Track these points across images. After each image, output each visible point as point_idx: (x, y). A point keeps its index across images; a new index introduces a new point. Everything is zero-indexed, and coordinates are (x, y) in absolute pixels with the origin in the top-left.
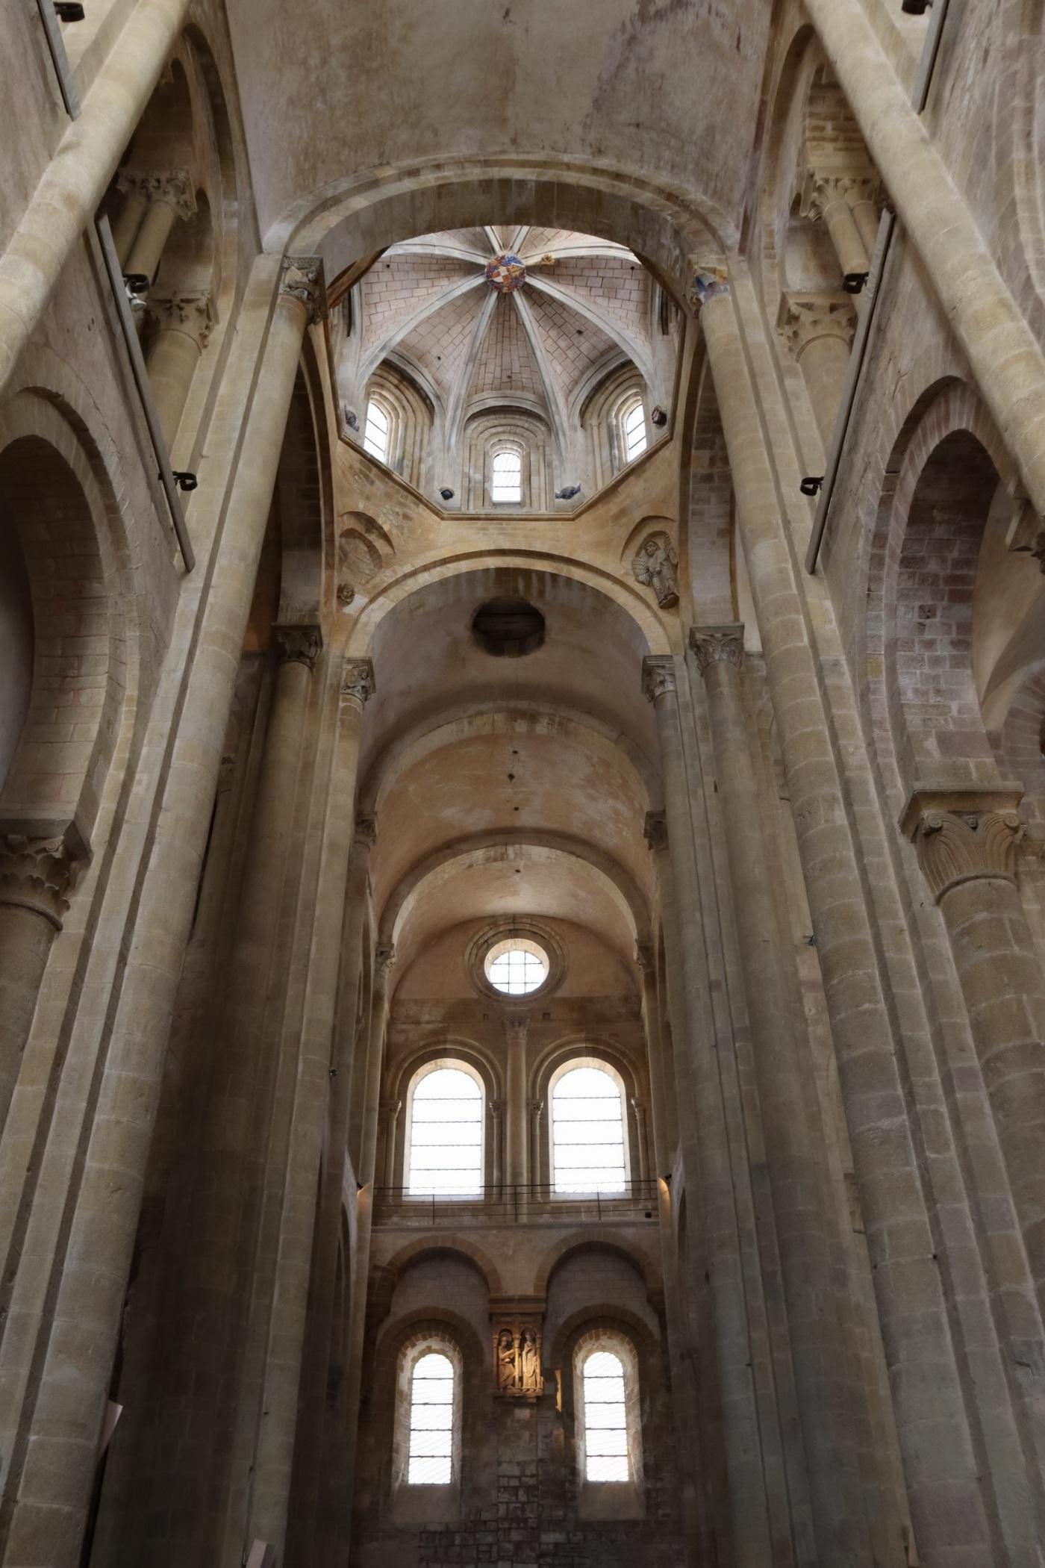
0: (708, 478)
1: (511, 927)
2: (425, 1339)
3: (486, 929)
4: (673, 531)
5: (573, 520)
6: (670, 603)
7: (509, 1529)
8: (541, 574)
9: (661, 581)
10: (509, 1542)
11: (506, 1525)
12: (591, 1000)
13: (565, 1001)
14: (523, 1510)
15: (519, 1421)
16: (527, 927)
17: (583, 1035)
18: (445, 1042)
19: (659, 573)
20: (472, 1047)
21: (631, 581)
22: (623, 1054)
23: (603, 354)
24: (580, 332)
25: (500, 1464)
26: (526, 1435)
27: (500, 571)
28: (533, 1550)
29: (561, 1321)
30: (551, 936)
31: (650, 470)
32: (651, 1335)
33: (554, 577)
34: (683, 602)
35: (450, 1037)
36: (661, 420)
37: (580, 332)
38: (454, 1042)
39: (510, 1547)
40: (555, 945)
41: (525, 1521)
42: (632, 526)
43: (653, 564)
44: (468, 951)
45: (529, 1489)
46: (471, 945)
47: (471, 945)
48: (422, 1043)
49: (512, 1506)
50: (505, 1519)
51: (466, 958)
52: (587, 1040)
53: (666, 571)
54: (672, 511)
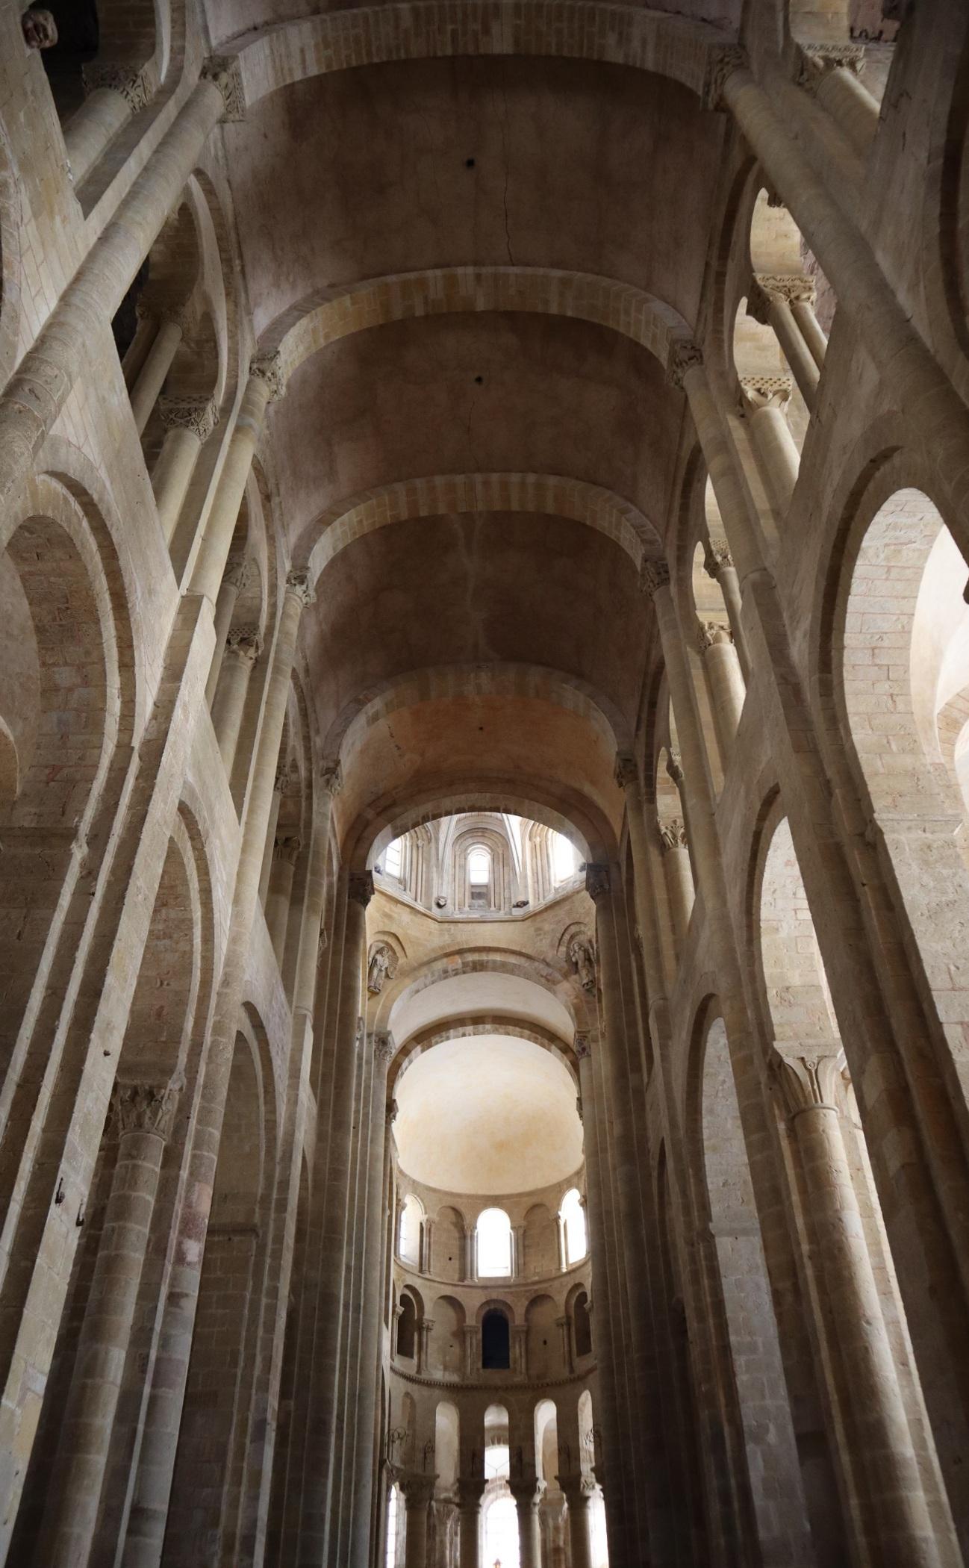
0: (445, 972)
31: (419, 919)
34: (376, 998)
36: (439, 906)
43: (379, 957)
54: (413, 954)
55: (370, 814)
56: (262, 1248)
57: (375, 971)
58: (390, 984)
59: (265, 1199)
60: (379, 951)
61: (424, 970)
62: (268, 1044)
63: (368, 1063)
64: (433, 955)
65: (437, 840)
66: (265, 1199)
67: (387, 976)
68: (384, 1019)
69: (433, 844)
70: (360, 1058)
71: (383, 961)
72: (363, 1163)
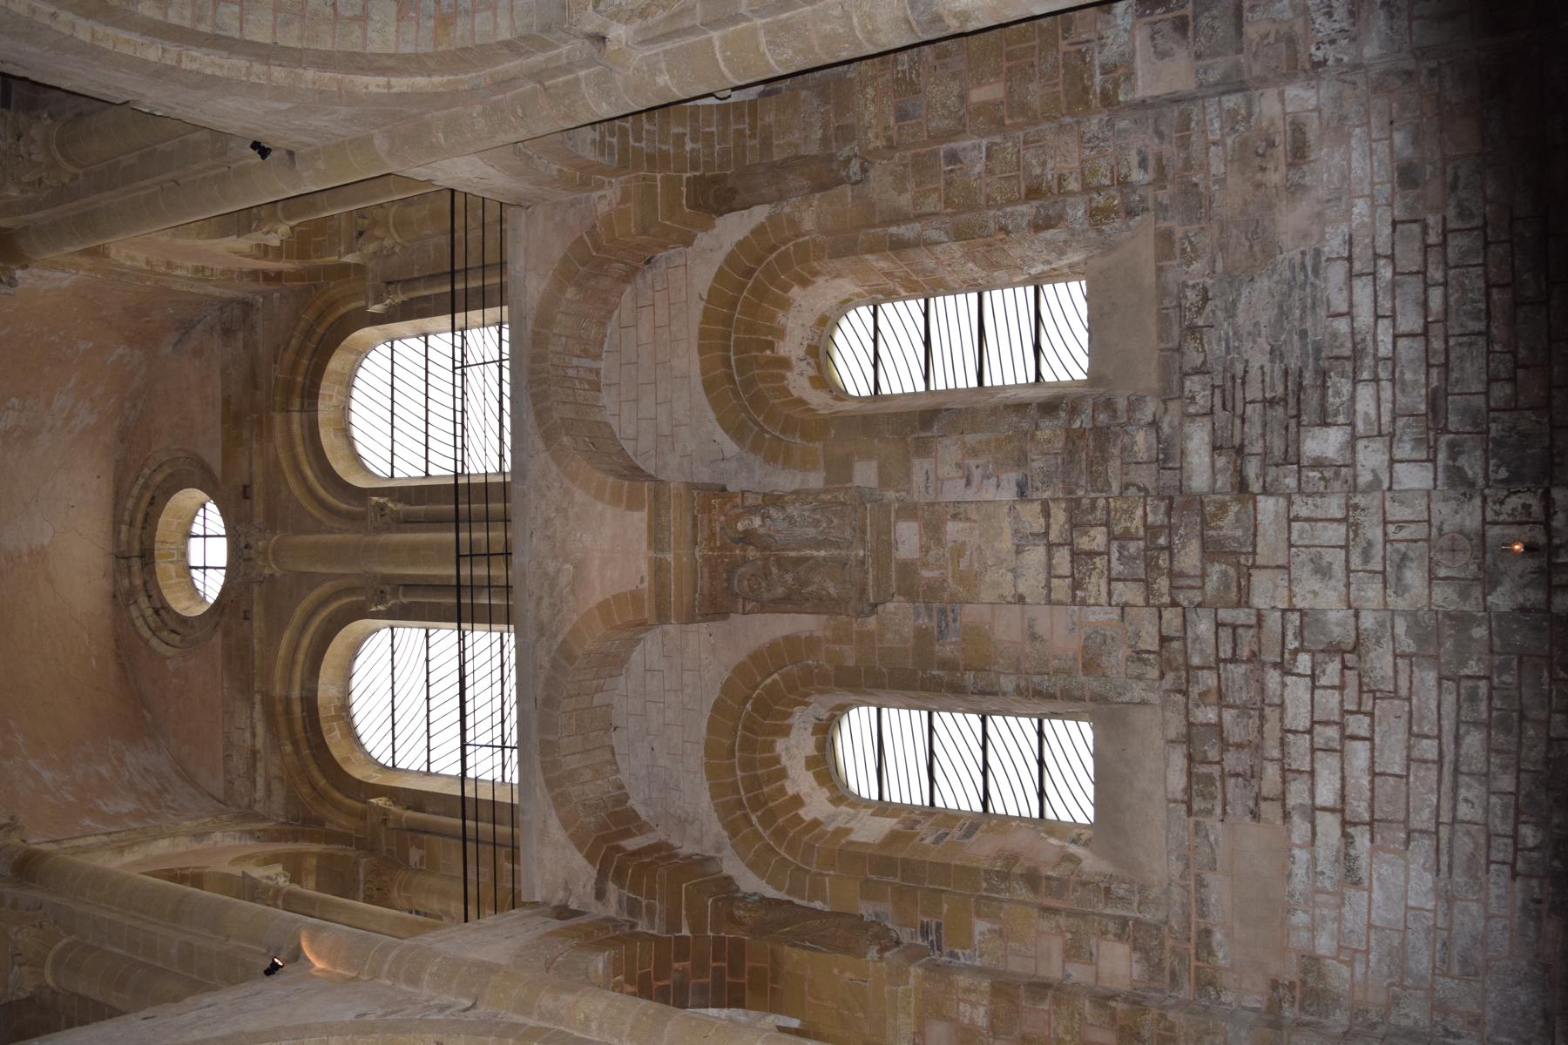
1: (136, 564)
2: (782, 774)
3: (134, 612)
7: (1172, 574)
10: (1204, 575)
11: (1163, 583)
12: (226, 402)
13: (227, 456)
14: (1127, 536)
15: (925, 550)
16: (137, 531)
17: (278, 418)
18: (288, 701)
20: (295, 648)
22: (309, 333)
25: (1021, 599)
26: (952, 527)
28: (1223, 507)
29: (731, 448)
30: (146, 486)
32: (759, 231)
35: (278, 690)
38: (289, 682)
39: (1215, 570)
40: (159, 478)
41: (1151, 531)
44: (163, 649)
45: (1076, 524)
46: (154, 642)
47: (154, 642)
48: (288, 748)
49: (1117, 567)
50: (1148, 584)
51: (169, 651)
52: (286, 409)
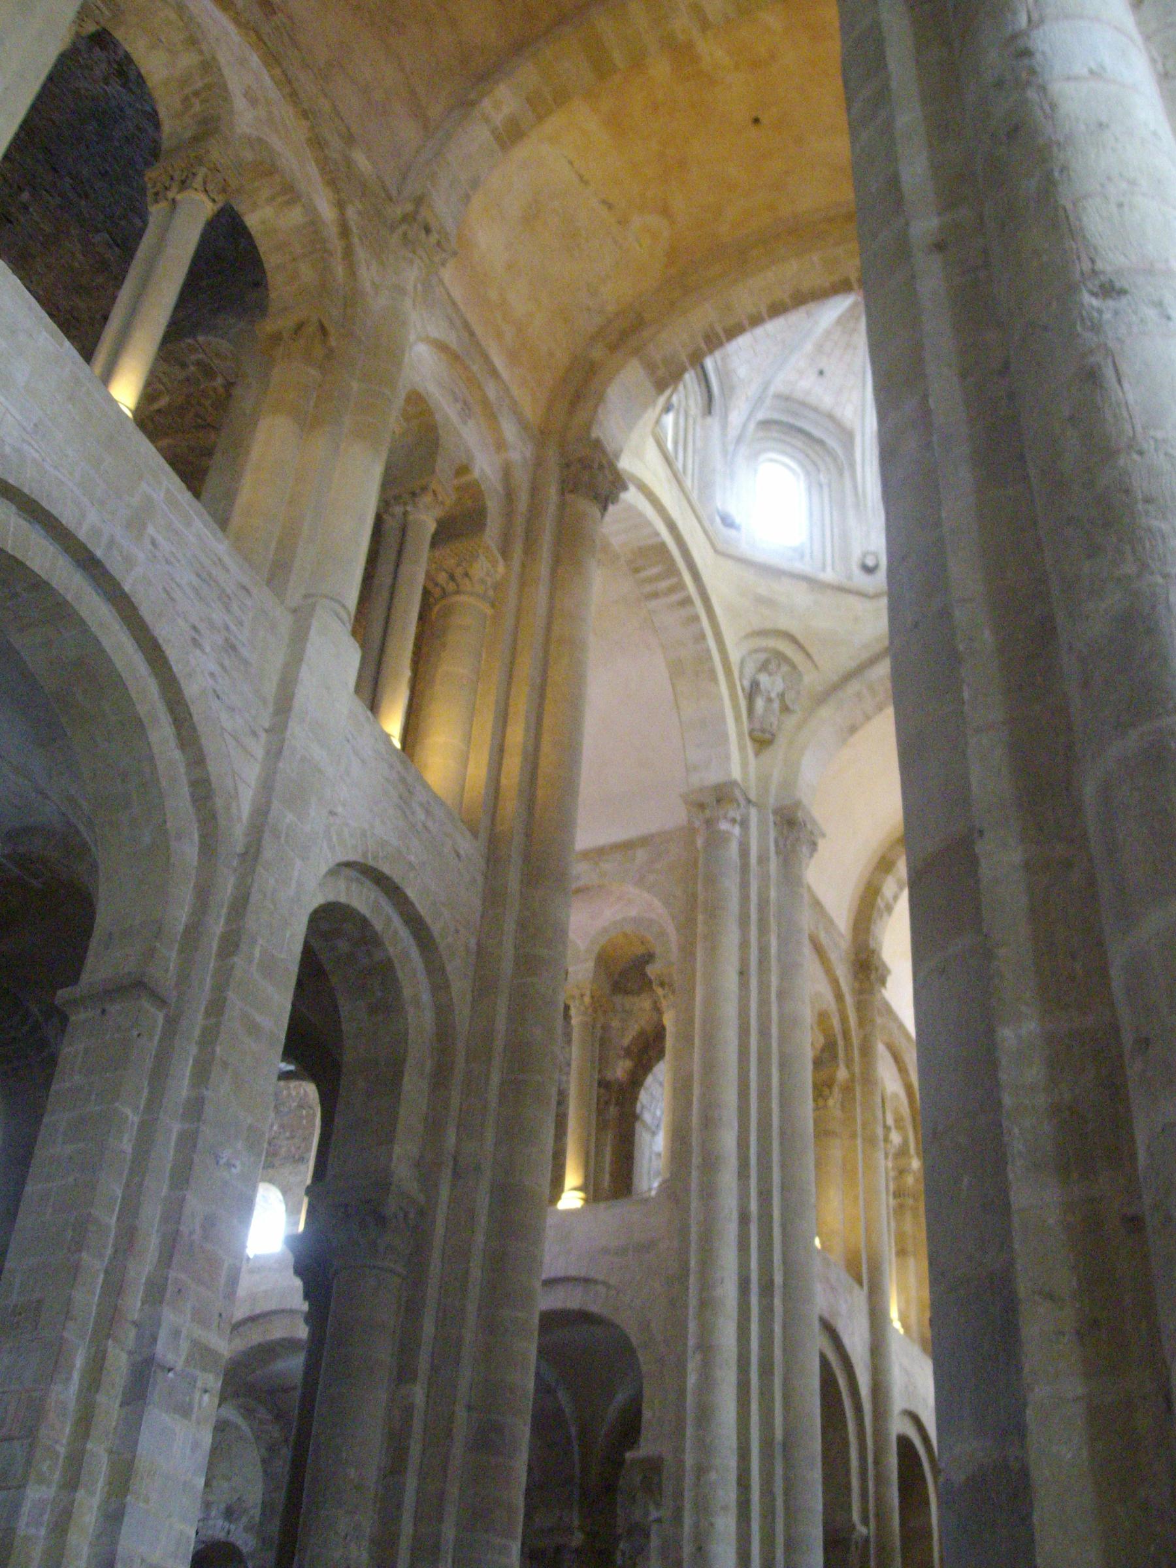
4: (811, 680)
5: (716, 551)
6: (762, 741)
8: (681, 586)
9: (766, 710)
19: (769, 700)
21: (736, 674)
23: (803, 404)
24: (821, 373)
27: (662, 548)
33: (687, 601)
37: (821, 373)
42: (768, 625)
43: (764, 679)
53: (776, 705)
54: (832, 663)
55: (597, 353)
56: (172, 1023)
57: (760, 703)
58: (791, 721)
59: (193, 932)
60: (764, 667)
61: (854, 687)
62: (135, 609)
63: (763, 860)
64: (865, 656)
65: (852, 465)
66: (193, 932)
67: (785, 709)
68: (789, 784)
69: (847, 474)
70: (744, 852)
71: (772, 684)
72: (764, 1033)
